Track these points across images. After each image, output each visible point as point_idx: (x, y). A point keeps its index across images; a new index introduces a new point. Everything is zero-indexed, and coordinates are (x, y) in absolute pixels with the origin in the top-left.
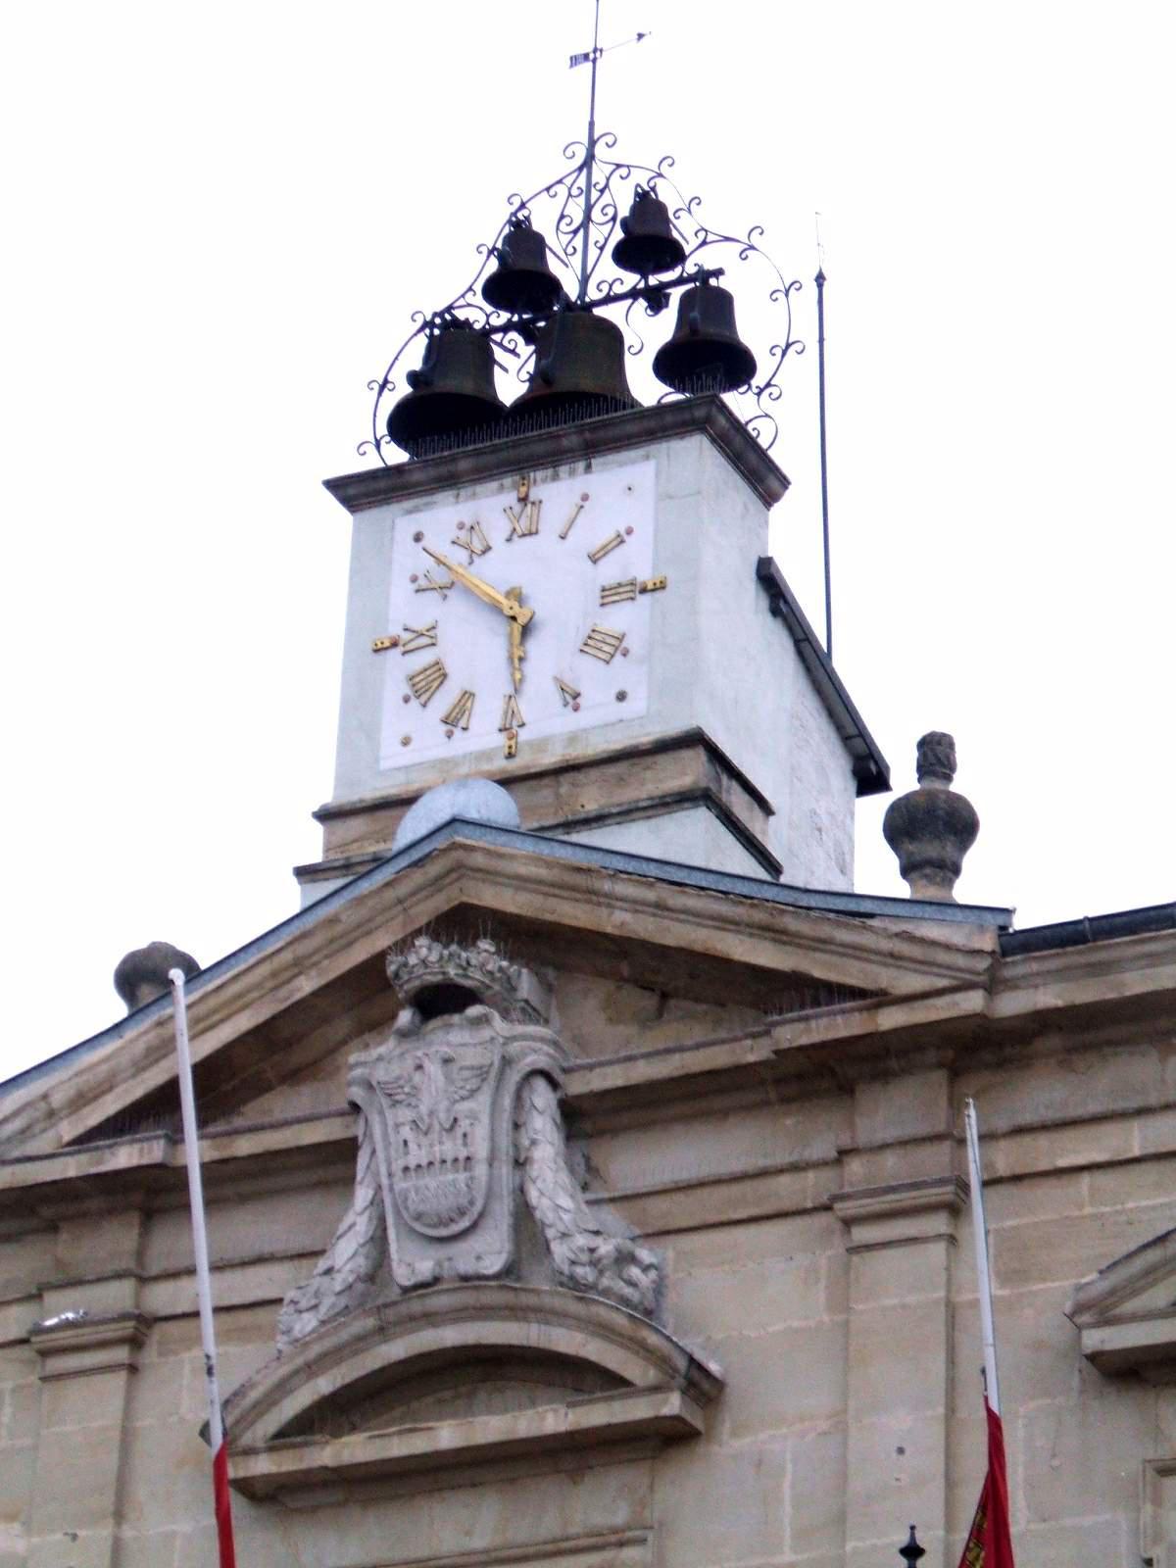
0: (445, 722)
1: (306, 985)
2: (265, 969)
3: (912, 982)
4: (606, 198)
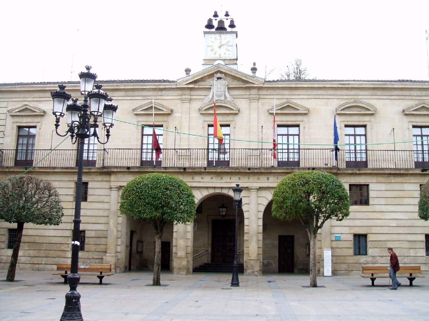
1: (206, 75)
3: (257, 83)
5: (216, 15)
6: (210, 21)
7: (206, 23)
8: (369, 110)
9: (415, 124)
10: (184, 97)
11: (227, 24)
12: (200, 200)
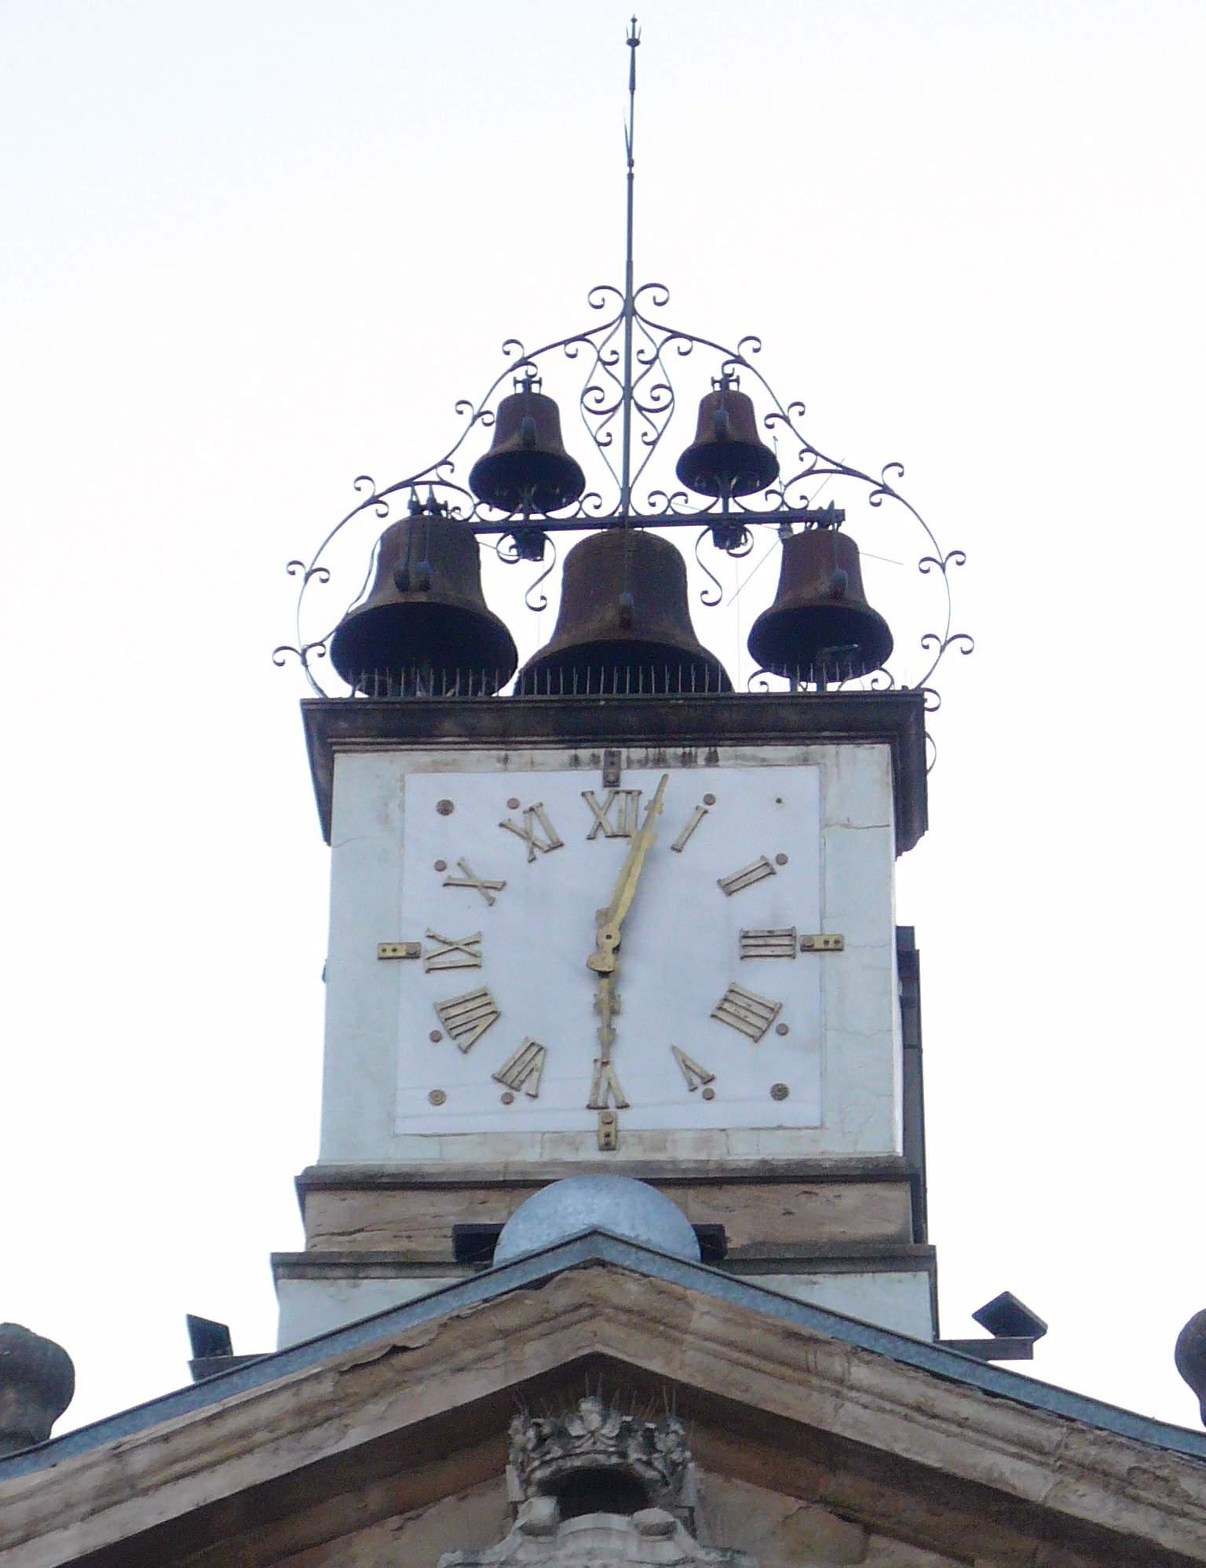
0: (499, 1079)
2: (286, 1401)
4: (656, 376)
6: (428, 556)
11: (728, 599)
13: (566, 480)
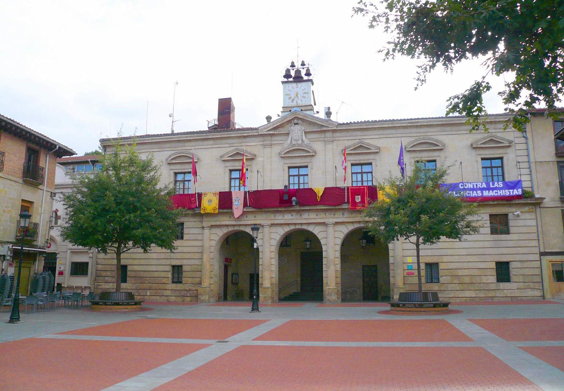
5: (293, 65)
6: (288, 71)
7: (284, 73)
8: (309, 152)
9: (353, 162)
10: (265, 143)
11: (303, 72)
12: (283, 235)
13: (295, 66)
